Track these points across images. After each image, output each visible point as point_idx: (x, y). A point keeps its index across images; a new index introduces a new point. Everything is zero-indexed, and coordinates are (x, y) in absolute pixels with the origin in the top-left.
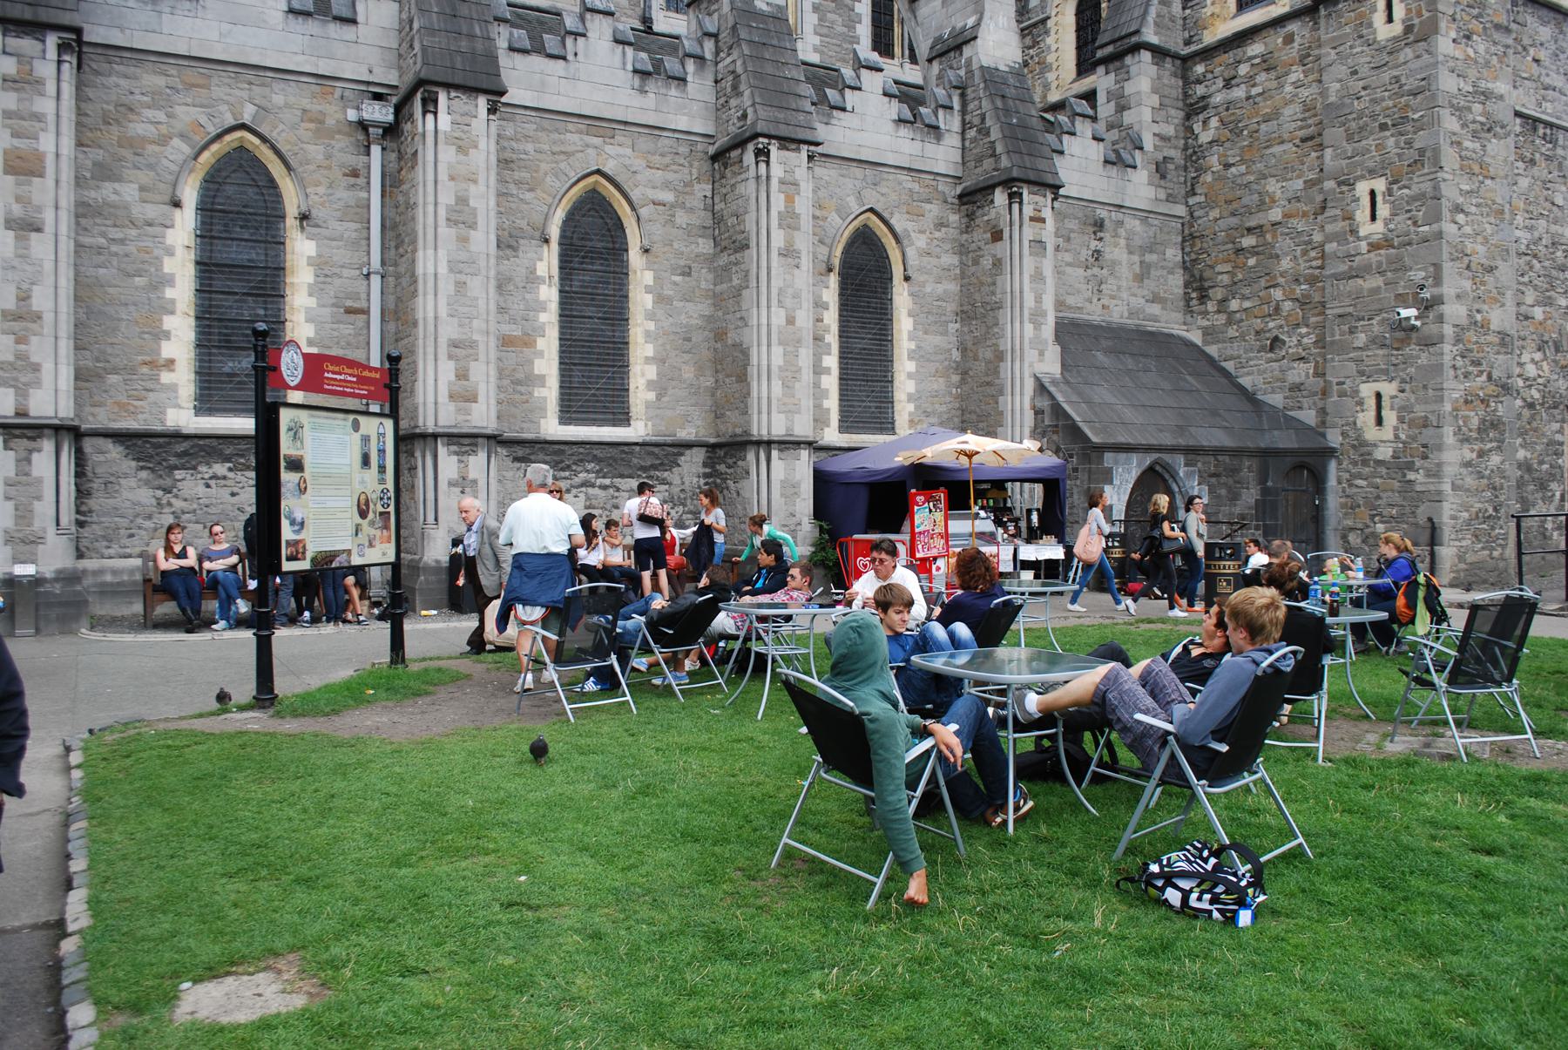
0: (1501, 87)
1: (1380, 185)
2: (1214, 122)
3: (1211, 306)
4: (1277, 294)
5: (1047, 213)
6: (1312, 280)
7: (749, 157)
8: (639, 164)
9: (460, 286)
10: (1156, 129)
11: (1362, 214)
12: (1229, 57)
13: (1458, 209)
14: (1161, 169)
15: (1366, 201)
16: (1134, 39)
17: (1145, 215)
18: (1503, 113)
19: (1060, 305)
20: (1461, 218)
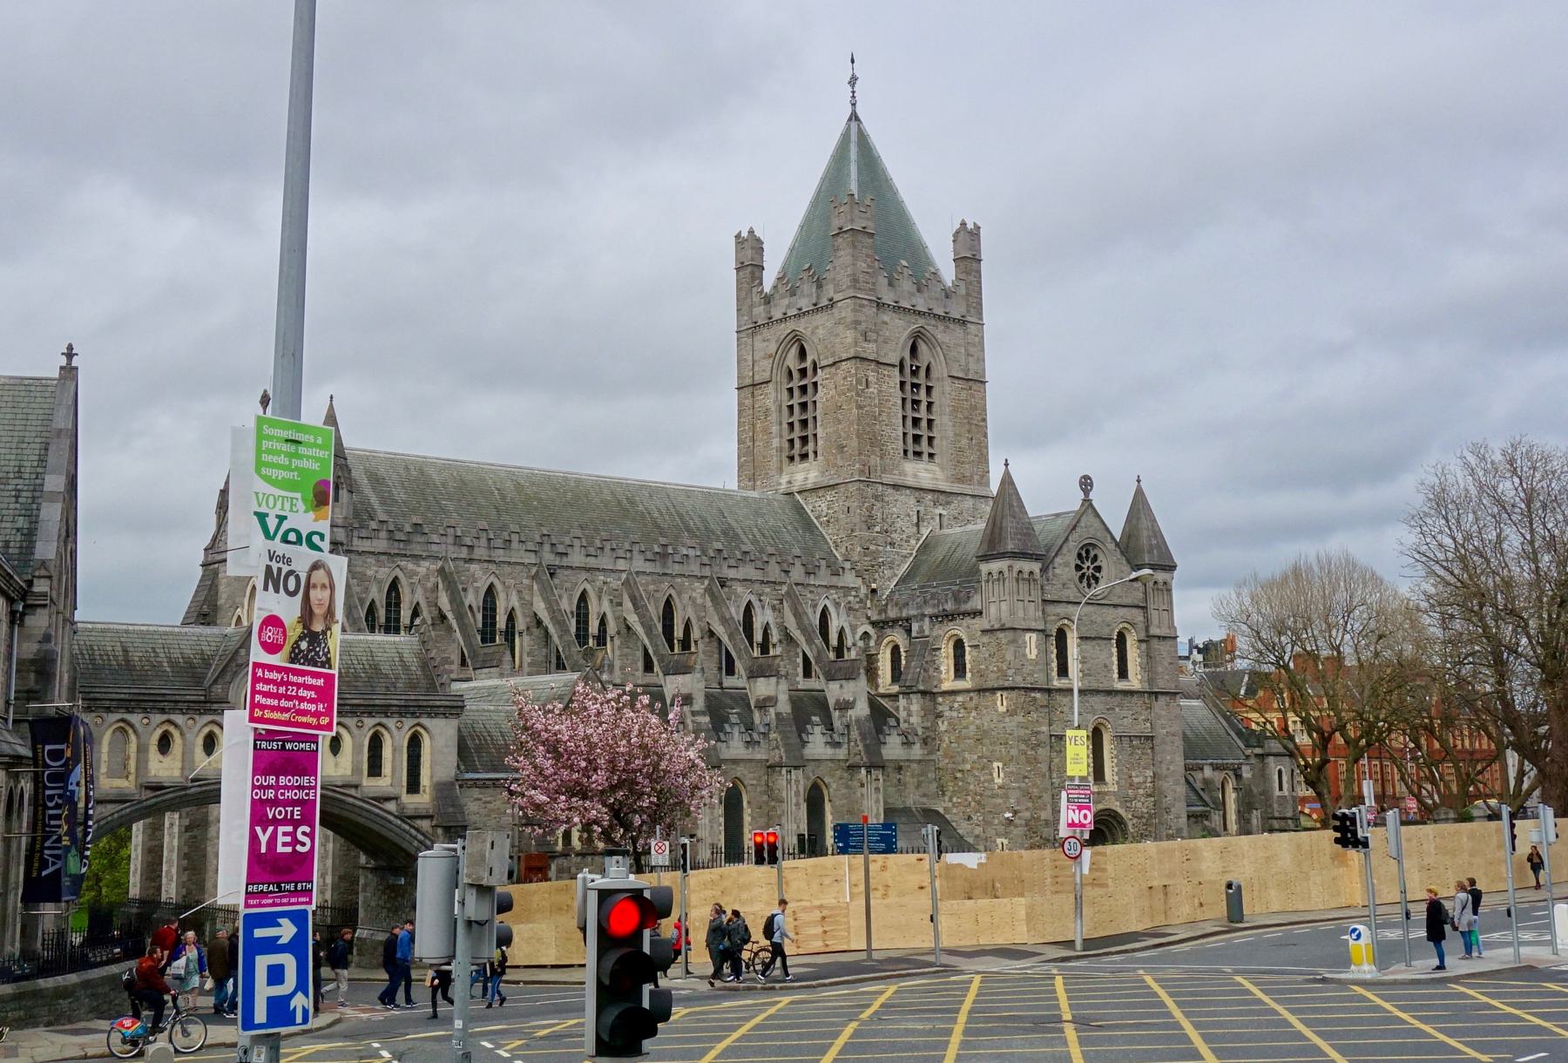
0: (1044, 729)
1: (1000, 765)
2: (946, 723)
3: (947, 798)
4: (970, 798)
5: (880, 777)
6: (981, 795)
7: (784, 771)
8: (746, 772)
9: (712, 827)
10: (923, 725)
11: (995, 775)
12: (952, 698)
13: (1025, 777)
14: (925, 742)
15: (996, 770)
16: (914, 689)
17: (920, 761)
18: (1043, 737)
19: (885, 803)
20: (1027, 780)
